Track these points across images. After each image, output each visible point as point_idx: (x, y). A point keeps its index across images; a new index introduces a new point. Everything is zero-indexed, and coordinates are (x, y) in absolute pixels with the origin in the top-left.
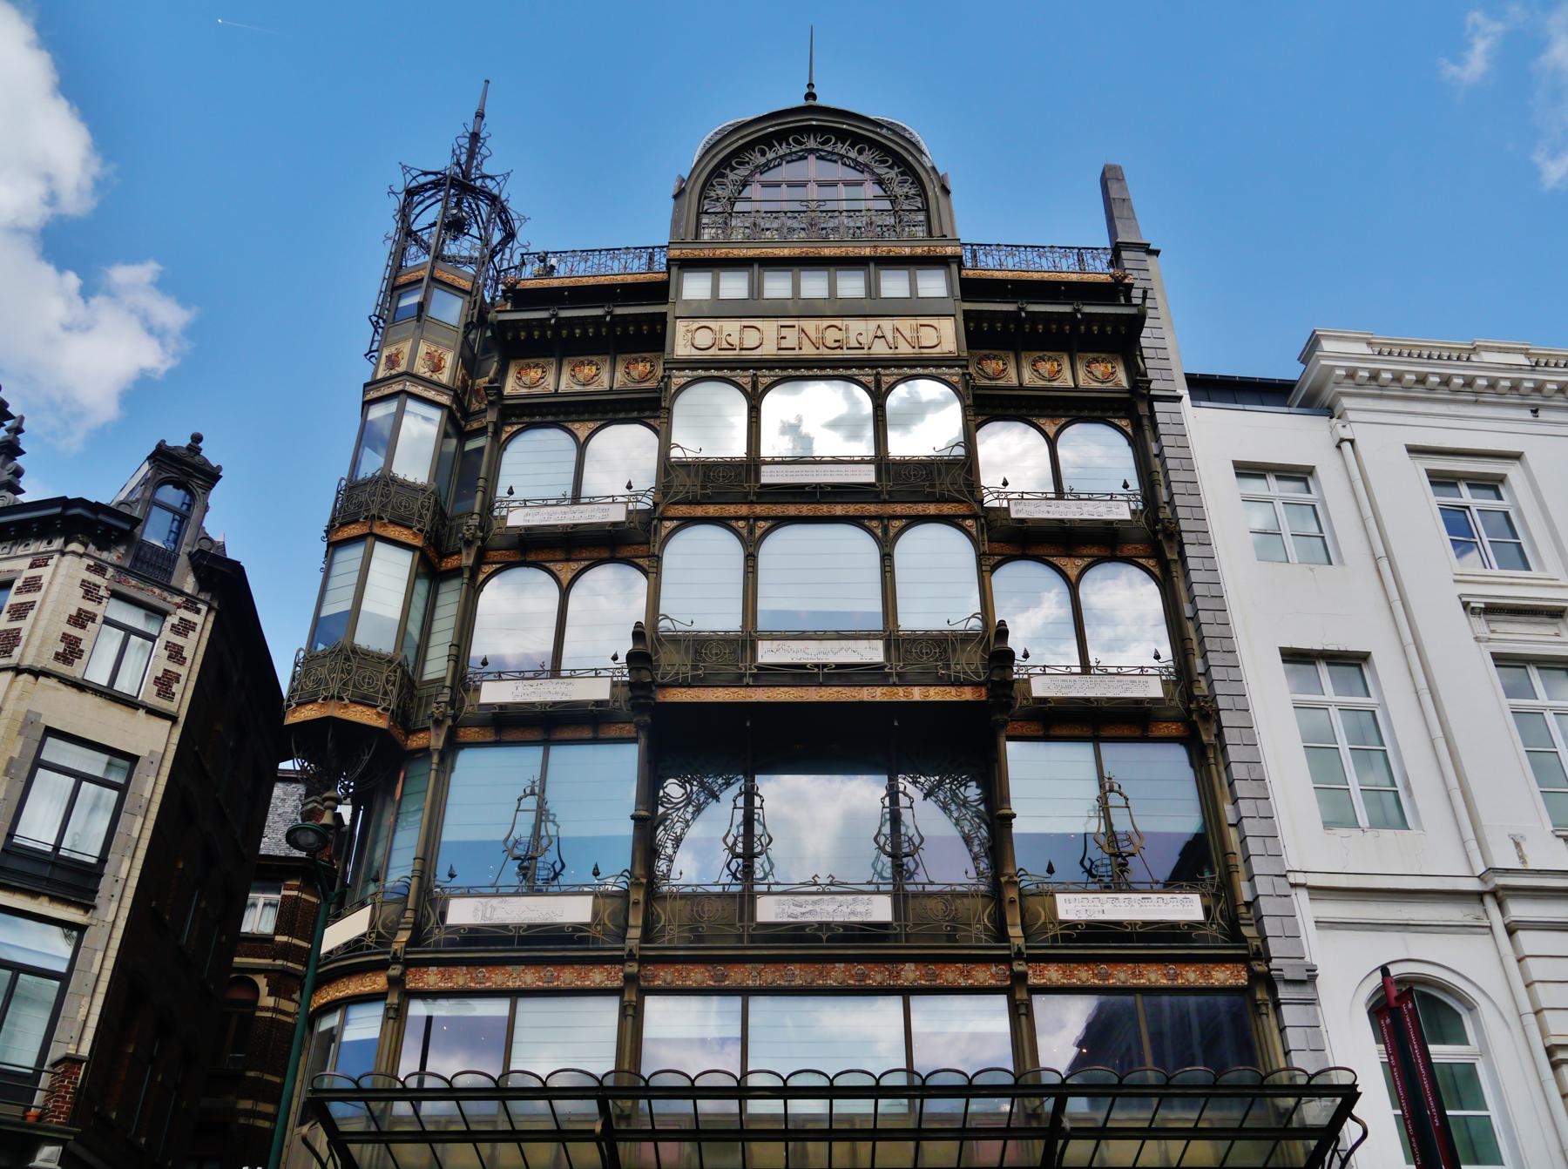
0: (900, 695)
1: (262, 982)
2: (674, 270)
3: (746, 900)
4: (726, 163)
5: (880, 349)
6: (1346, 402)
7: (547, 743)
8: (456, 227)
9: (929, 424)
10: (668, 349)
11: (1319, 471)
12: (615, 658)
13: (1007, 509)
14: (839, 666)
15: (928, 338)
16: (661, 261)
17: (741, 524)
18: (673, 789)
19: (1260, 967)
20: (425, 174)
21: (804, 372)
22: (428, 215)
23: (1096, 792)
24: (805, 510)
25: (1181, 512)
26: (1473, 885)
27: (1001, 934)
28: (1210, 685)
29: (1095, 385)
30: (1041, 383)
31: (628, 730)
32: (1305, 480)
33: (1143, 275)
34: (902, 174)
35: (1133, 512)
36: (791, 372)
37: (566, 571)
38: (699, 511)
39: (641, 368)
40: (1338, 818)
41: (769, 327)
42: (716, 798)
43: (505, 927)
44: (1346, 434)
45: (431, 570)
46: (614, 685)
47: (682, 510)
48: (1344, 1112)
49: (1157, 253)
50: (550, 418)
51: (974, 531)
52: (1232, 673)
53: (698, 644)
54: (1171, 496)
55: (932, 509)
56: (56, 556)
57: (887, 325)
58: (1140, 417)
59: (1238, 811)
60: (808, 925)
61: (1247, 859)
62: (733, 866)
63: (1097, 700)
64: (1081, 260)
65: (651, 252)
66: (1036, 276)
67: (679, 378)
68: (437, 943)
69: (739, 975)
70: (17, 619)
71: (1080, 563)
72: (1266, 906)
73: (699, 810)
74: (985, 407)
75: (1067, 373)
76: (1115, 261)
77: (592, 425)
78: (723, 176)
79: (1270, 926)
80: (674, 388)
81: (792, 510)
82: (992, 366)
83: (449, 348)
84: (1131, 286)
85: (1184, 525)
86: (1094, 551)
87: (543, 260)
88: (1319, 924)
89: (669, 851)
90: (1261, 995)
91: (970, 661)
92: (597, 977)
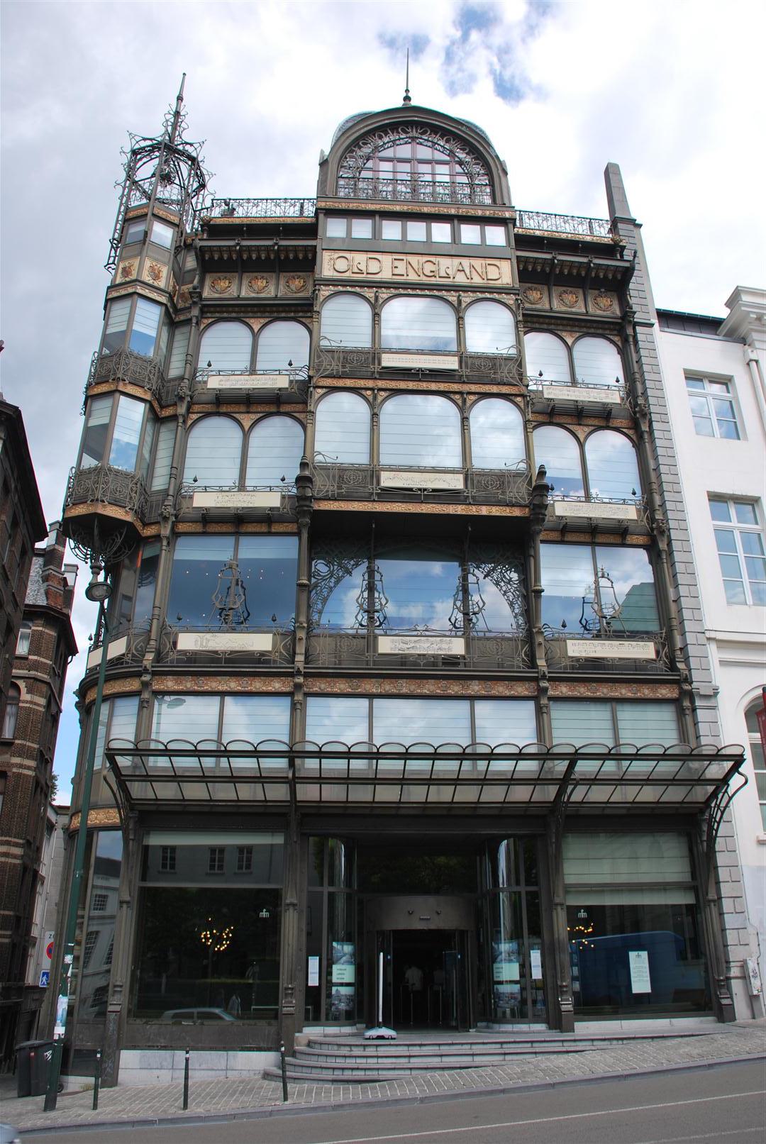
0: (474, 510)
1: (22, 684)
2: (321, 216)
3: (371, 641)
4: (356, 143)
5: (461, 279)
6: (755, 336)
7: (237, 534)
8: (166, 178)
9: (490, 332)
10: (317, 268)
11: (736, 379)
12: (283, 480)
13: (542, 392)
14: (434, 490)
15: (493, 273)
16: (310, 210)
17: (369, 392)
18: (321, 567)
19: (686, 687)
20: (145, 139)
21: (410, 292)
22: (146, 170)
23: (592, 578)
24: (411, 385)
25: (651, 401)
27: (532, 663)
28: (665, 513)
29: (599, 312)
30: (564, 309)
31: (292, 527)
32: (726, 384)
33: (631, 240)
34: (476, 159)
35: (622, 399)
36: (402, 291)
37: (247, 420)
38: (340, 383)
39: (297, 283)
40: (733, 598)
41: (387, 259)
42: (350, 573)
43: (216, 652)
44: (753, 356)
45: (156, 418)
46: (283, 497)
47: (328, 382)
48: (735, 769)
49: (640, 226)
50: (234, 315)
51: (522, 405)
52: (679, 506)
53: (341, 472)
54: (645, 389)
55: (495, 389)
57: (466, 262)
58: (627, 336)
59: (678, 592)
60: (412, 655)
61: (682, 622)
62: (360, 618)
63: (597, 519)
64: (591, 227)
65: (301, 202)
66: (564, 236)
67: (325, 292)
68: (172, 661)
69: (369, 686)
71: (587, 430)
72: (692, 650)
73: (339, 580)
74: (530, 322)
75: (581, 303)
76: (614, 228)
77: (263, 321)
78: (352, 151)
79: (694, 663)
80: (322, 298)
81: (402, 385)
82: (534, 295)
83: (165, 264)
84: (623, 248)
85: (653, 409)
86: (596, 422)
87: (227, 204)
89: (320, 606)
90: (686, 703)
91: (520, 491)
92: (277, 685)
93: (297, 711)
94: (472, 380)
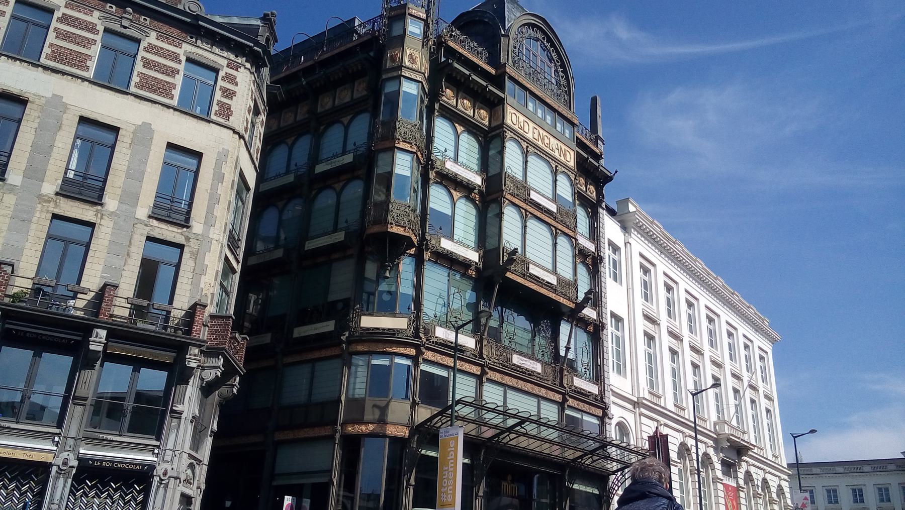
5: (556, 154)
24: (539, 214)
26: (636, 400)
37: (456, 195)
41: (532, 125)
44: (631, 240)
47: (509, 197)
55: (567, 231)
56: (242, 68)
57: (560, 144)
69: (508, 380)
70: (226, 97)
88: (614, 403)
93: (480, 384)
94: (558, 223)
